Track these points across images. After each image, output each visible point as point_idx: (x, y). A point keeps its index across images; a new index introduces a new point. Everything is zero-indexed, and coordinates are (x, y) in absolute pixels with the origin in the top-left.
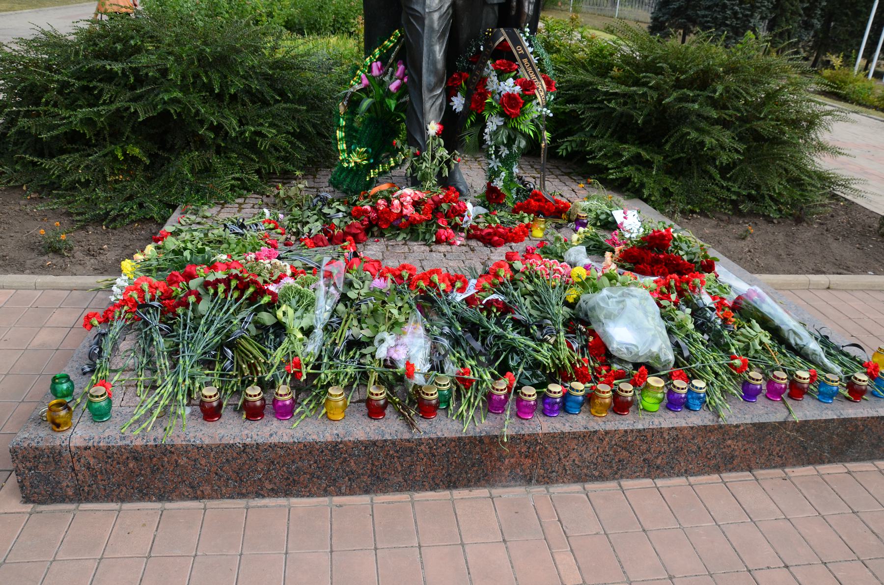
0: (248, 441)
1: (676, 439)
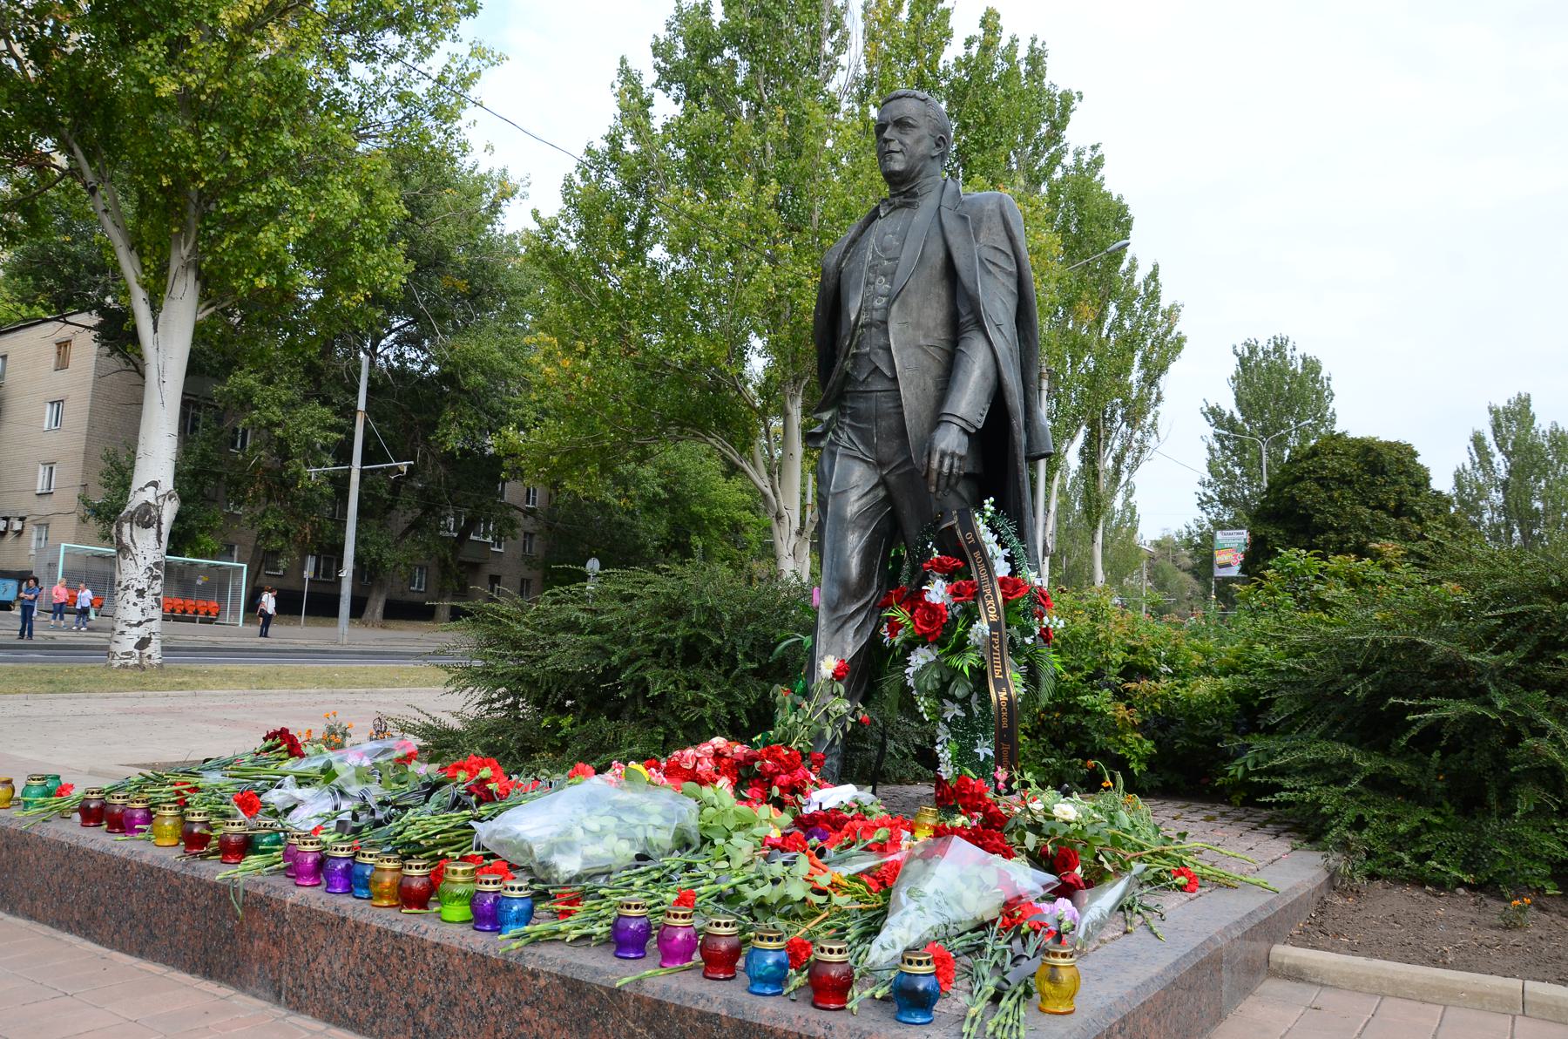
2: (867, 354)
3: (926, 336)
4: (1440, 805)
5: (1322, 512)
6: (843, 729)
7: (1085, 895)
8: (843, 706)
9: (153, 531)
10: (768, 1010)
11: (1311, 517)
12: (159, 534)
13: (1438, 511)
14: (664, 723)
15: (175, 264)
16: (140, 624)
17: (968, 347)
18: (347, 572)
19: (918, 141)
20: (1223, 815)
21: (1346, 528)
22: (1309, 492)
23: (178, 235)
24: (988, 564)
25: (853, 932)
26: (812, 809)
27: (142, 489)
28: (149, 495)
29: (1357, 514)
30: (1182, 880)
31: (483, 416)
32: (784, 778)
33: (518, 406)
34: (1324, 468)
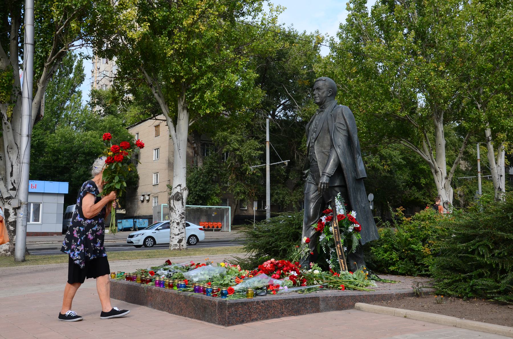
9: (180, 202)
12: (183, 203)
15: (180, 108)
16: (178, 234)
18: (268, 207)
19: (323, 93)
23: (179, 97)
27: (176, 188)
28: (178, 190)
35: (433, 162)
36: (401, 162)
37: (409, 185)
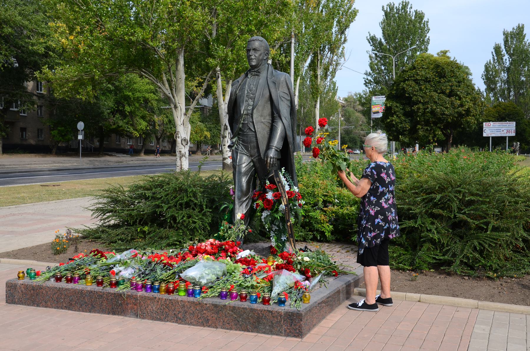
0: (60, 287)
1: (184, 306)
2: (247, 124)
3: (264, 119)
4: (408, 248)
5: (416, 96)
6: (244, 233)
7: (312, 279)
8: (243, 227)
10: (255, 306)
11: (411, 98)
13: (468, 94)
14: (181, 229)
17: (277, 124)
20: (352, 250)
21: (427, 103)
22: (411, 87)
24: (283, 187)
25: (266, 291)
26: (239, 258)
29: (432, 96)
30: (334, 274)
31: (12, 48)
32: (231, 250)
33: (33, 45)
34: (418, 75)
35: (174, 97)
36: (110, 88)
37: (113, 113)
